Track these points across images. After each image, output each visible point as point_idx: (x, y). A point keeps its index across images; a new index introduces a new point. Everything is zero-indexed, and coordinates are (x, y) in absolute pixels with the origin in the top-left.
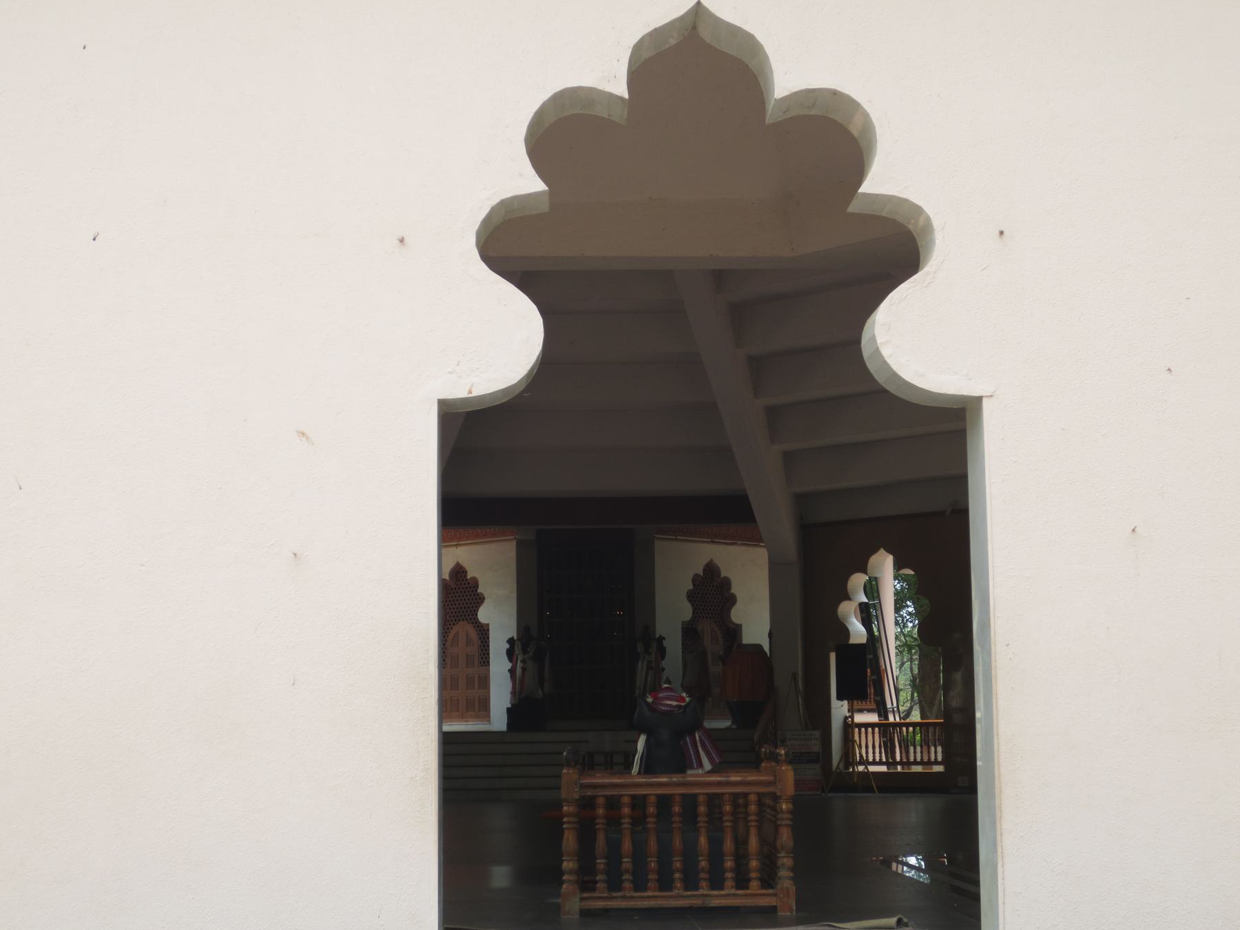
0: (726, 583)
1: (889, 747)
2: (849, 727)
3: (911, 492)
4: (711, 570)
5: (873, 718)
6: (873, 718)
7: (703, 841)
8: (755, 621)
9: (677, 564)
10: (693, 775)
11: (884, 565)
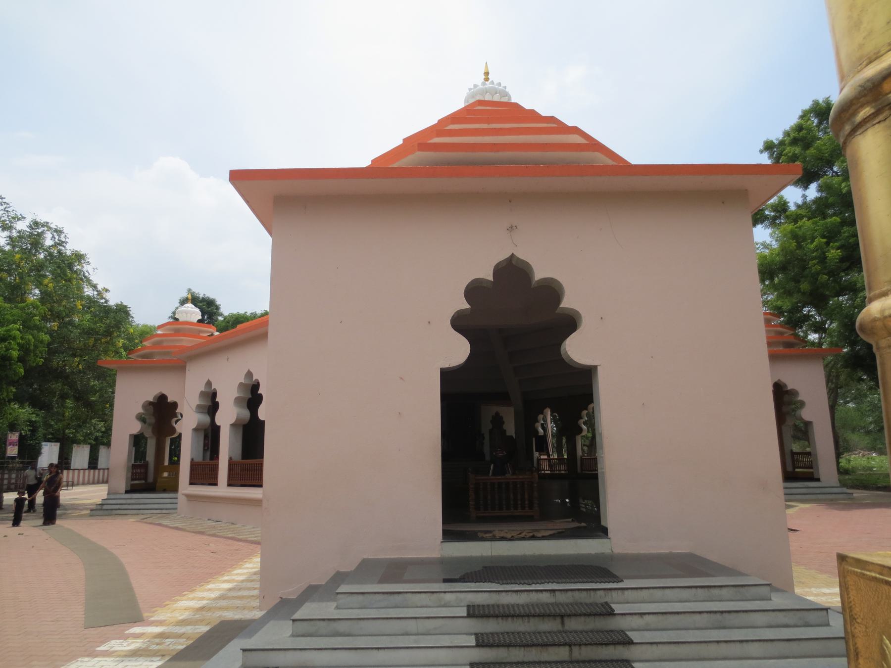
0: (502, 418)
1: (550, 466)
2: (539, 460)
3: (576, 392)
4: (497, 414)
5: (546, 457)
6: (546, 457)
7: (512, 496)
8: (510, 429)
9: (488, 412)
10: (508, 476)
11: (548, 412)
